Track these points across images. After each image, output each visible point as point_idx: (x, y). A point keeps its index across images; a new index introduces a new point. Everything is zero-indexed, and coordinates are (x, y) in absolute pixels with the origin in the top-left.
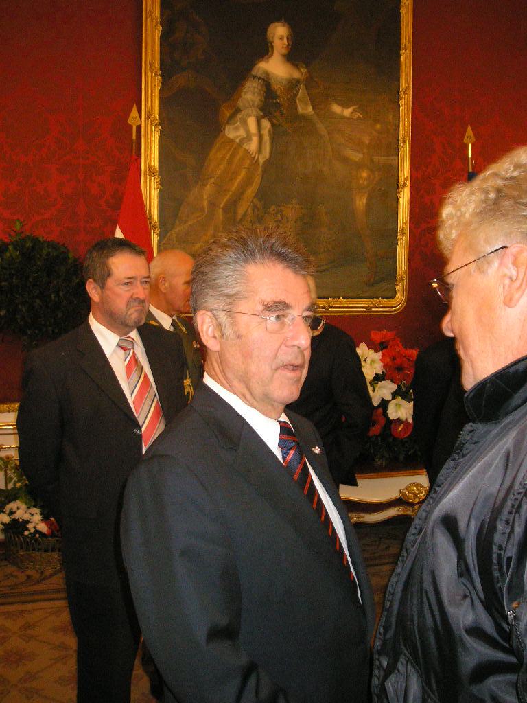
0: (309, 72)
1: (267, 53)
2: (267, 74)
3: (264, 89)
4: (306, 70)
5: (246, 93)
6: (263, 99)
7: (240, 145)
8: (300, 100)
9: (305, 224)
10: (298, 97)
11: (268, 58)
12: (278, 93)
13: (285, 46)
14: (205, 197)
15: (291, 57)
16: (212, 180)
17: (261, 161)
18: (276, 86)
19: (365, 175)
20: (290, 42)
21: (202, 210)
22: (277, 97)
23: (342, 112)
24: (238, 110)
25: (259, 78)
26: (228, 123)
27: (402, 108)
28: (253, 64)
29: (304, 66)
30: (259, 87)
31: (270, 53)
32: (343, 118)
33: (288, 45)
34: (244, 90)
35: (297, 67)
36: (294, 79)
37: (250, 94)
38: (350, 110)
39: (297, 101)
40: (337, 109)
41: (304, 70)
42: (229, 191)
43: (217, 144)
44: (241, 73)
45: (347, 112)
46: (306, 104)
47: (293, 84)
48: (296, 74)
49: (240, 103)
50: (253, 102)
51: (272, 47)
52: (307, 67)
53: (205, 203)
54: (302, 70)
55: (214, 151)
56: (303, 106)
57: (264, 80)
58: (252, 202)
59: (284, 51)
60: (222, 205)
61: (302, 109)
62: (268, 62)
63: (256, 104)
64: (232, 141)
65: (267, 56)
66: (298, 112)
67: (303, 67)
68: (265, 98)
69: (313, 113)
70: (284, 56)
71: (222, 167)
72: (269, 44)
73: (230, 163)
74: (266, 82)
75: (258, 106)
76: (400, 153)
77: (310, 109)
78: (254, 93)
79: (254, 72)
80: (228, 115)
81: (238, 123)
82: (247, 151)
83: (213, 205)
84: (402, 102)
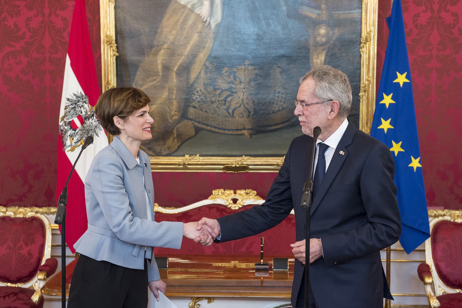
7: (192, 10)
9: (259, 84)
14: (159, 61)
16: (165, 46)
17: (213, 25)
19: (323, 31)
21: (157, 74)
42: (182, 55)
53: (160, 67)
58: (205, 65)
60: (175, 69)
64: (184, 7)
71: (174, 32)
73: (182, 28)
82: (199, 16)
83: (167, 68)
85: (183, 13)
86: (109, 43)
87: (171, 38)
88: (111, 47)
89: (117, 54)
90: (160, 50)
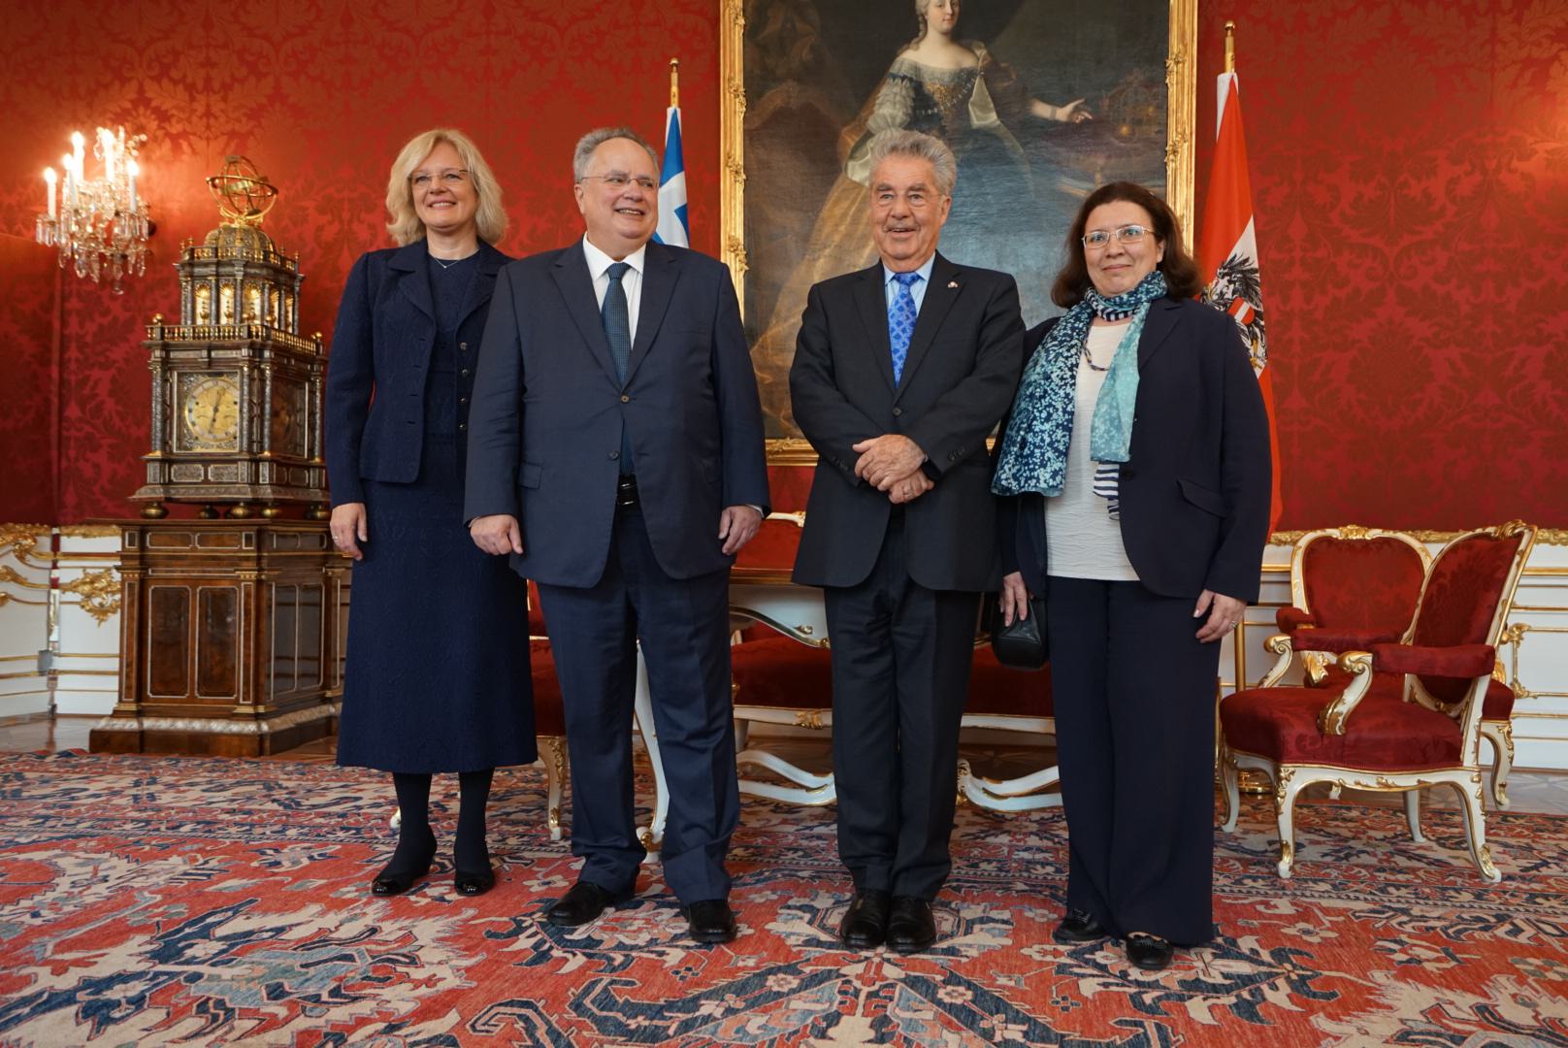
0: (990, 53)
1: (917, 36)
2: (917, 69)
3: (912, 94)
4: (984, 52)
5: (881, 104)
6: (910, 111)
8: (973, 104)
10: (972, 99)
11: (918, 43)
12: (937, 97)
13: (948, 17)
15: (957, 35)
16: (827, 251)
18: (930, 87)
20: (957, 9)
22: (936, 104)
23: (1054, 113)
24: (869, 135)
25: (903, 78)
26: (852, 157)
27: (1173, 91)
28: (891, 56)
29: (983, 45)
30: (904, 92)
31: (921, 34)
32: (1056, 123)
33: (953, 15)
34: (878, 101)
35: (969, 49)
36: (962, 70)
37: (889, 105)
38: (1070, 107)
39: (970, 108)
40: (1042, 110)
41: (981, 52)
43: (834, 193)
44: (875, 71)
45: (1062, 114)
46: (984, 108)
47: (962, 80)
48: (968, 62)
49: (871, 123)
50: (893, 118)
51: (925, 22)
52: (986, 47)
54: (978, 53)
55: (828, 206)
56: (979, 113)
57: (911, 80)
59: (946, 26)
61: (978, 119)
62: (917, 49)
63: (898, 121)
65: (915, 40)
66: (970, 126)
67: (980, 48)
68: (914, 109)
69: (998, 122)
70: (945, 34)
71: (842, 228)
72: (920, 19)
74: (916, 86)
75: (900, 125)
76: (1169, 172)
77: (992, 118)
78: (895, 104)
79: (895, 69)
80: (852, 144)
81: (869, 156)
84: (1172, 80)
85: (859, 194)
86: (734, 248)
87: (837, 238)
88: (737, 255)
89: (747, 268)
90: (819, 258)
